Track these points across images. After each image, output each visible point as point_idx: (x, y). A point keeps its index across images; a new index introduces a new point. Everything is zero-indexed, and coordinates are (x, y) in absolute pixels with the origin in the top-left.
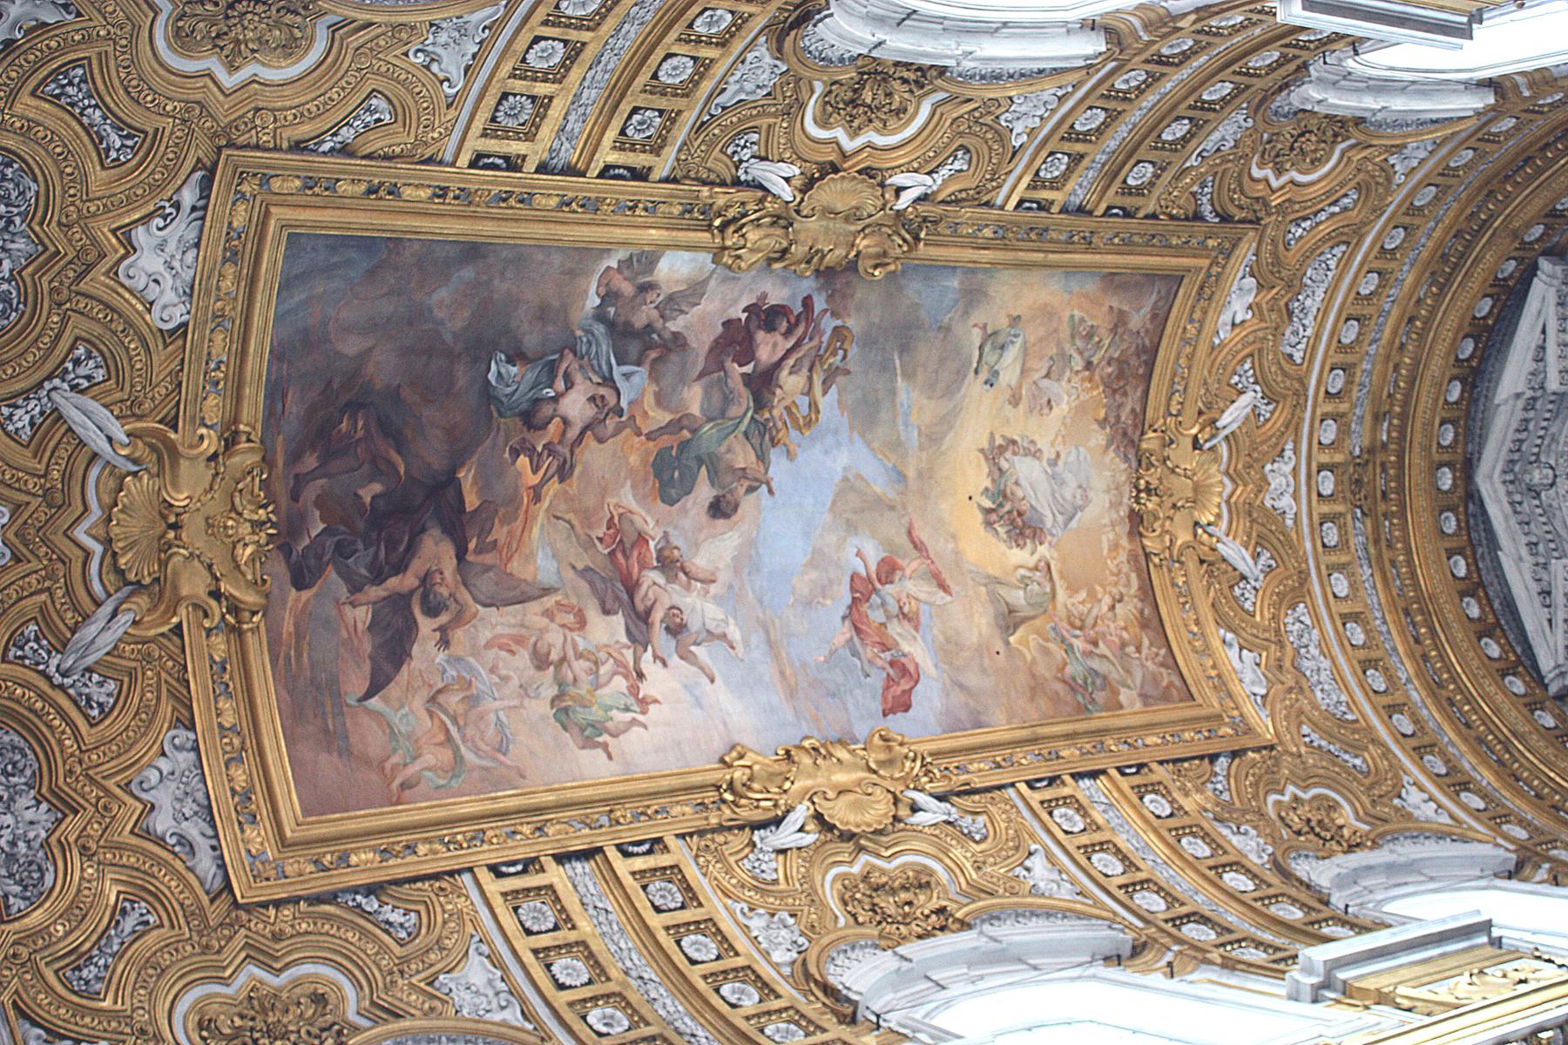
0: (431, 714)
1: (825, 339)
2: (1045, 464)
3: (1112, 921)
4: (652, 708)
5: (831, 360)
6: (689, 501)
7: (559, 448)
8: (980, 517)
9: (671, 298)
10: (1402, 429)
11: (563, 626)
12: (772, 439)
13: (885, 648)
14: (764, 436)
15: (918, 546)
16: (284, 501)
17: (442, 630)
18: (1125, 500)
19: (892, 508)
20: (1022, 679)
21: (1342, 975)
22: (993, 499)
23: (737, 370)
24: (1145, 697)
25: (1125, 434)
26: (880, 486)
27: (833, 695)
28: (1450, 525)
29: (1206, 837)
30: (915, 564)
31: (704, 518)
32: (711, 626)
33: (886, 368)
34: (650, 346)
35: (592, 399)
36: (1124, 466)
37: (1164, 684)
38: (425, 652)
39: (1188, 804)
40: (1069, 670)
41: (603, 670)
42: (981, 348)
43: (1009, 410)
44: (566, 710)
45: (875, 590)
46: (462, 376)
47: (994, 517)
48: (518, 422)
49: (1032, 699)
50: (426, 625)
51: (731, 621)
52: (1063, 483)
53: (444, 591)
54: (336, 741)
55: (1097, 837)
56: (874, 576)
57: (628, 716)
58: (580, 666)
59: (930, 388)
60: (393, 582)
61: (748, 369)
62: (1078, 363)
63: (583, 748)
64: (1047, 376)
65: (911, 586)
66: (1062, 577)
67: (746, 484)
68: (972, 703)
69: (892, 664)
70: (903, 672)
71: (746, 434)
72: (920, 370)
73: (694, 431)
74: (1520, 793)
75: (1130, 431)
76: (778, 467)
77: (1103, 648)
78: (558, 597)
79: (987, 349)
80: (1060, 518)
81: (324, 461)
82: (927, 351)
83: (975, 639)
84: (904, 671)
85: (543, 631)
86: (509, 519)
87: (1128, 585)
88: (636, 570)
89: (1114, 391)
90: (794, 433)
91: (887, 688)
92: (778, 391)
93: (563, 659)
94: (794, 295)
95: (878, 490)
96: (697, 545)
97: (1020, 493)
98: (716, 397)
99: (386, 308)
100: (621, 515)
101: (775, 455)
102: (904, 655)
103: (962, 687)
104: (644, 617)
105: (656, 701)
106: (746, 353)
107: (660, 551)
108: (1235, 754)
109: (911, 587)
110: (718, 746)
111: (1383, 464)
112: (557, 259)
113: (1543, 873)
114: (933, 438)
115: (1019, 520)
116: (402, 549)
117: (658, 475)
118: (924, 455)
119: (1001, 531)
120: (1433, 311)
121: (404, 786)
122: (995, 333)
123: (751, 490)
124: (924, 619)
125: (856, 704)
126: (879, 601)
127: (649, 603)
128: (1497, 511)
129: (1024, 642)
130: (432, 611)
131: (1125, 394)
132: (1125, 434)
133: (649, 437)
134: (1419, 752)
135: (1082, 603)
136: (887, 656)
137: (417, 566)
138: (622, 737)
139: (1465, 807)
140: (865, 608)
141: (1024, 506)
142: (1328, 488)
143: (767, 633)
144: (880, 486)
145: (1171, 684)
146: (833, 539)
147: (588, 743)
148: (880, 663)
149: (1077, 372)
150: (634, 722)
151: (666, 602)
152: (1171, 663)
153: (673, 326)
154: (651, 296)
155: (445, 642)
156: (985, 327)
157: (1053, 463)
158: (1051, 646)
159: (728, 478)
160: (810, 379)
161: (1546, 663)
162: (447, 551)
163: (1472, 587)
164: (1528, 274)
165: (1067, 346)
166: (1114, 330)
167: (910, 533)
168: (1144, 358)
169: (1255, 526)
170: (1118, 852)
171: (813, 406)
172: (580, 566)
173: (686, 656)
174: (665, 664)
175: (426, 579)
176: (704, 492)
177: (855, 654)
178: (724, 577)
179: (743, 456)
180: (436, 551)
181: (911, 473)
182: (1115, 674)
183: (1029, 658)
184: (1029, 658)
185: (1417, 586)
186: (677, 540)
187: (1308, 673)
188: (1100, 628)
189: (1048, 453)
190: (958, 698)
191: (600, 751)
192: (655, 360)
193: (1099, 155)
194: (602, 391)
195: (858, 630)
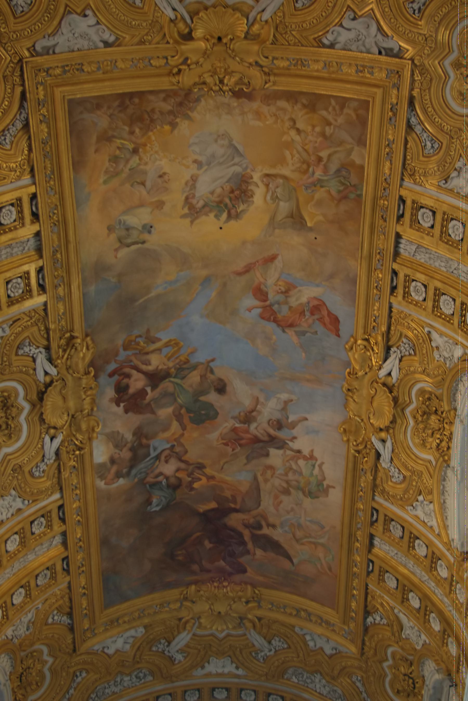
0: (302, 544)
1: (129, 353)
4: (316, 454)
5: (142, 343)
7: (190, 470)
8: (232, 222)
9: (116, 446)
11: (272, 476)
12: (185, 363)
13: (302, 313)
15: (248, 269)
18: (226, 100)
19: (225, 285)
22: (221, 212)
23: (150, 394)
25: (181, 104)
30: (258, 275)
32: (280, 407)
34: (141, 445)
35: (167, 462)
36: (203, 102)
37: (354, 117)
40: (334, 193)
41: (294, 467)
42: (128, 246)
43: (166, 208)
45: (271, 306)
47: (233, 212)
50: (266, 531)
51: (278, 396)
52: (213, 156)
56: (262, 304)
57: (317, 467)
61: (149, 389)
62: (135, 161)
63: (327, 496)
64: (143, 184)
65: (271, 281)
67: (209, 375)
69: (312, 314)
71: (183, 378)
75: (179, 99)
77: (324, 154)
79: (129, 241)
80: (237, 160)
87: (284, 110)
88: (249, 436)
89: (152, 121)
91: (324, 324)
92: (160, 367)
93: (287, 482)
95: (214, 294)
97: (219, 191)
100: (223, 439)
101: (193, 361)
102: (308, 303)
103: (331, 276)
105: (312, 451)
106: (142, 393)
107: (241, 422)
115: (237, 193)
116: (232, 533)
121: (330, 569)
122: (120, 241)
123: (212, 372)
126: (276, 306)
127: (265, 434)
130: (260, 527)
131: (153, 110)
135: (293, 156)
136: (307, 314)
137: (241, 528)
138: (326, 476)
140: (279, 316)
141: (227, 188)
145: (355, 110)
148: (310, 321)
149: (140, 159)
150: (320, 466)
151: (265, 425)
153: (129, 436)
154: (116, 456)
155: (274, 526)
158: (317, 196)
160: (153, 352)
162: (234, 516)
165: (124, 175)
167: (239, 274)
168: (127, 102)
171: (167, 345)
172: (245, 461)
173: (293, 426)
174: (295, 438)
175: (247, 526)
177: (303, 333)
181: (204, 273)
183: (321, 218)
184: (321, 218)
189: (193, 169)
194: (163, 458)
195: (291, 326)
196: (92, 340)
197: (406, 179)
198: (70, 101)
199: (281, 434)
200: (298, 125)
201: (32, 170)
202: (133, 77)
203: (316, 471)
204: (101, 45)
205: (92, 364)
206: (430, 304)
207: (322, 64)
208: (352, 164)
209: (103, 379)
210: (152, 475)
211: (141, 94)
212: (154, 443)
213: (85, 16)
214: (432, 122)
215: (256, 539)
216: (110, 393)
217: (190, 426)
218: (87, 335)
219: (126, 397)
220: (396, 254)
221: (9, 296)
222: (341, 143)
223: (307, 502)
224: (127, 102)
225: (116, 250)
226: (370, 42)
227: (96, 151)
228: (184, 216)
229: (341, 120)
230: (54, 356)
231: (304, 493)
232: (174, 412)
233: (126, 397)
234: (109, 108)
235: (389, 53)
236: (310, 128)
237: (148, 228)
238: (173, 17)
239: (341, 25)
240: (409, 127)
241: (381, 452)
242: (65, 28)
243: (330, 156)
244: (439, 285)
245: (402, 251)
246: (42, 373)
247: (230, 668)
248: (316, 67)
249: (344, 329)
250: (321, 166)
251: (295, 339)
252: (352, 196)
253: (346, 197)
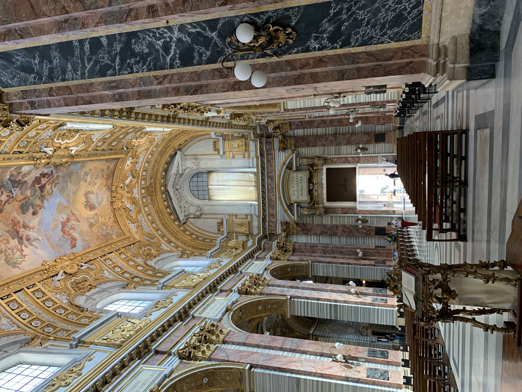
3: (122, 281)
6: (28, 213)
9: (24, 174)
10: (155, 180)
13: (70, 235)
14: (42, 198)
15: (73, 214)
21: (165, 284)
23: (37, 186)
24: (117, 236)
26: (65, 204)
28: (164, 196)
29: (133, 261)
32: (35, 237)
33: (66, 182)
35: (7, 196)
39: (128, 255)
41: (14, 251)
43: (89, 186)
44: (8, 261)
55: (115, 265)
58: (9, 251)
61: (40, 185)
62: (101, 176)
65: (73, 222)
70: (74, 239)
73: (28, 199)
74: (179, 242)
77: (108, 228)
78: (3, 238)
82: (74, 177)
84: (74, 239)
90: (49, 196)
91: (71, 243)
93: (6, 250)
96: (30, 222)
98: (33, 192)
101: (45, 202)
103: (85, 240)
104: (21, 238)
106: (39, 182)
107: (23, 224)
108: (134, 244)
109: (73, 222)
110: (41, 262)
113: (186, 256)
114: (75, 193)
117: (21, 209)
120: (160, 160)
123: (40, 209)
124: (76, 228)
128: (171, 193)
133: (20, 201)
134: (163, 237)
139: (171, 246)
140: (65, 228)
142: (143, 192)
144: (65, 204)
146: (57, 215)
150: (23, 261)
151: (25, 234)
153: (24, 179)
154: (20, 174)
157: (97, 194)
161: (181, 219)
163: (168, 207)
164: (176, 153)
166: (107, 169)
170: (119, 267)
171: (52, 191)
173: (31, 245)
176: (31, 210)
177: (64, 238)
178: (36, 227)
179: (38, 202)
181: (71, 200)
182: (111, 232)
185: (159, 207)
186: (26, 221)
189: (96, 193)
190: (84, 242)
191: (17, 268)
193: (108, 142)
195: (64, 233)
199: (25, 241)
203: (20, 260)
217: (20, 203)
251: (61, 235)
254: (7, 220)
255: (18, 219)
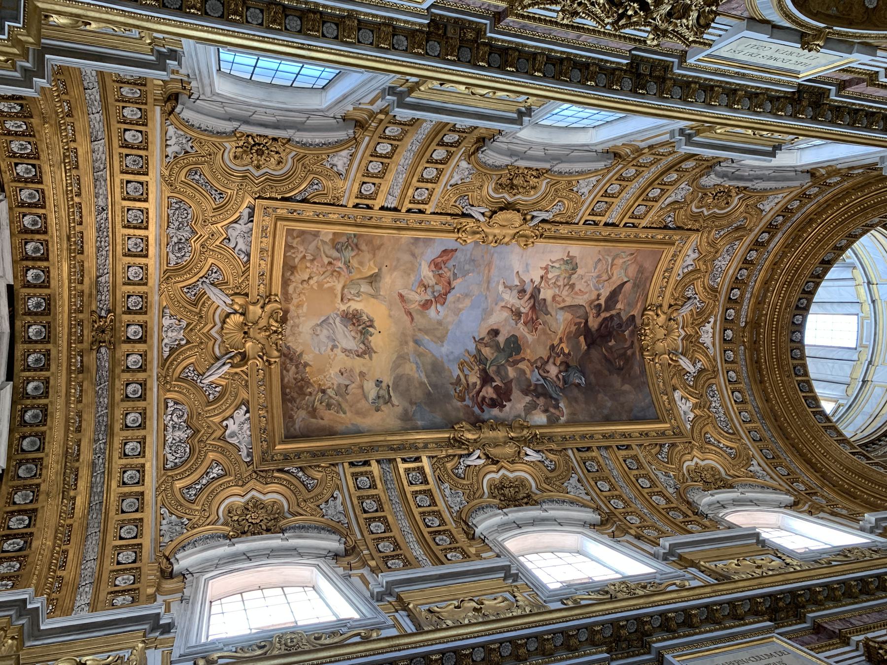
1: (467, 397)
2: (340, 346)
4: (544, 266)
6: (507, 336)
8: (375, 324)
9: (535, 408)
13: (440, 275)
14: (480, 359)
15: (409, 314)
16: (636, 341)
17: (598, 299)
18: (289, 328)
19: (419, 330)
20: (381, 254)
22: (368, 332)
23: (498, 383)
25: (291, 360)
26: (426, 338)
27: (473, 260)
30: (413, 306)
31: (501, 329)
32: (509, 291)
33: (435, 386)
34: (535, 390)
35: (548, 372)
38: (605, 293)
42: (390, 397)
43: (364, 370)
45: (435, 298)
46: (592, 378)
47: (368, 324)
48: (571, 364)
49: (382, 245)
50: (602, 301)
53: (594, 311)
54: (641, 270)
56: (434, 303)
59: (409, 380)
60: (608, 315)
61: (494, 384)
62: (329, 391)
64: (347, 386)
65: (417, 298)
66: (336, 296)
68: (413, 248)
69: (441, 268)
70: (436, 265)
72: (417, 385)
73: (508, 361)
75: (288, 361)
76: (472, 347)
77: (326, 260)
79: (387, 396)
80: (331, 321)
81: (625, 354)
83: (395, 274)
85: (567, 296)
86: (570, 332)
89: (302, 380)
90: (467, 360)
93: (565, 286)
94: (489, 412)
95: (426, 337)
96: (506, 320)
97: (353, 333)
98: (503, 373)
99: (622, 399)
101: (474, 352)
103: (413, 255)
104: (532, 296)
106: (496, 389)
107: (520, 319)
109: (416, 297)
111: (82, 342)
112: (581, 418)
114: (401, 358)
118: (406, 350)
119: (365, 317)
121: (632, 254)
123: (483, 339)
124: (417, 284)
125: (466, 255)
129: (370, 268)
130: (599, 305)
131: (295, 379)
132: (291, 360)
133: (524, 359)
135: (328, 282)
136: (440, 272)
137: (600, 319)
141: (351, 327)
143: (488, 287)
144: (426, 338)
145: (294, 238)
146: (449, 319)
147: (572, 258)
148: (446, 270)
149: (329, 388)
150: (553, 262)
151: (522, 302)
152: (288, 247)
153: (528, 399)
154: (542, 408)
155: (599, 295)
156: (393, 405)
158: (356, 265)
159: (492, 344)
160: (467, 381)
162: (590, 324)
165: (340, 399)
167: (412, 319)
168: (289, 397)
169: (197, 310)
171: (462, 371)
173: (523, 282)
175: (598, 315)
176: (501, 339)
177: (455, 275)
178: (498, 308)
179: (487, 352)
180: (594, 323)
181: (411, 344)
184: (372, 263)
187: (188, 228)
188: (322, 270)
189: (338, 351)
190: (417, 251)
192: (530, 386)
194: (545, 375)
195: (449, 283)
196: (456, 424)
197: (341, 203)
198: (286, 437)
199: (529, 290)
200: (306, 279)
201: (333, 465)
202: (271, 393)
203: (557, 265)
204: (248, 415)
205: (473, 424)
206: (430, 186)
207: (262, 262)
208: (333, 240)
209: (485, 416)
210: (558, 383)
211: (283, 387)
212: (533, 380)
213: (227, 426)
214: (300, 185)
215: (608, 308)
216: (495, 411)
217: (522, 355)
218: (453, 427)
219: (499, 400)
220: (395, 209)
221: (421, 483)
222: (318, 248)
223: (580, 271)
224: (289, 397)
225: (393, 405)
226: (244, 228)
227: (322, 419)
228: (371, 358)
229: (301, 249)
230: (466, 452)
231: (573, 274)
232: (511, 366)
233: (499, 400)
234: (292, 410)
235: (251, 215)
236: (308, 270)
237: (378, 383)
238: (229, 365)
239: (234, 248)
240: (304, 201)
241: (540, 219)
242: (234, 441)
243: (327, 256)
244: (415, 179)
245: (393, 206)
246: (478, 460)
247: (708, 327)
248: (263, 266)
249: (452, 245)
250: (335, 262)
251: (459, 281)
252: (355, 240)
253: (356, 245)
254: (544, 332)
255: (526, 330)
